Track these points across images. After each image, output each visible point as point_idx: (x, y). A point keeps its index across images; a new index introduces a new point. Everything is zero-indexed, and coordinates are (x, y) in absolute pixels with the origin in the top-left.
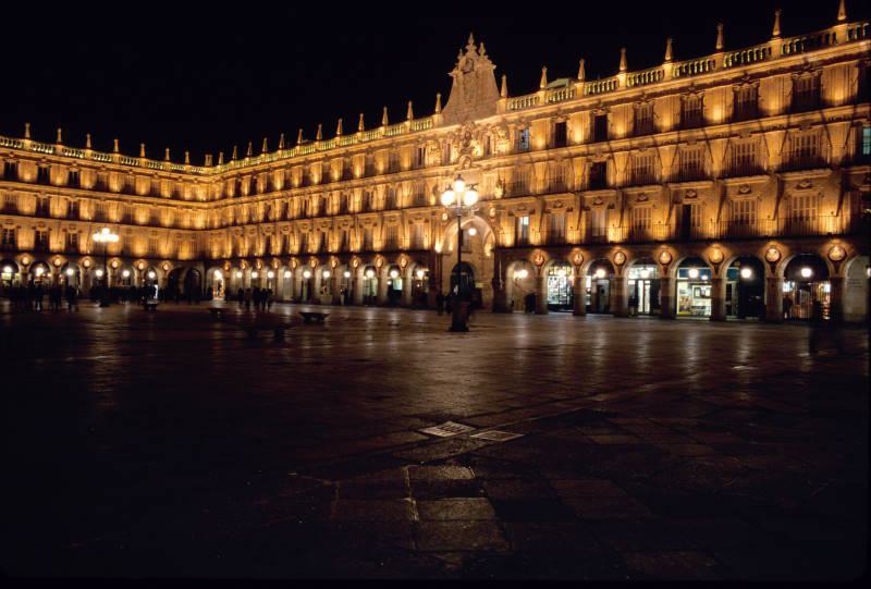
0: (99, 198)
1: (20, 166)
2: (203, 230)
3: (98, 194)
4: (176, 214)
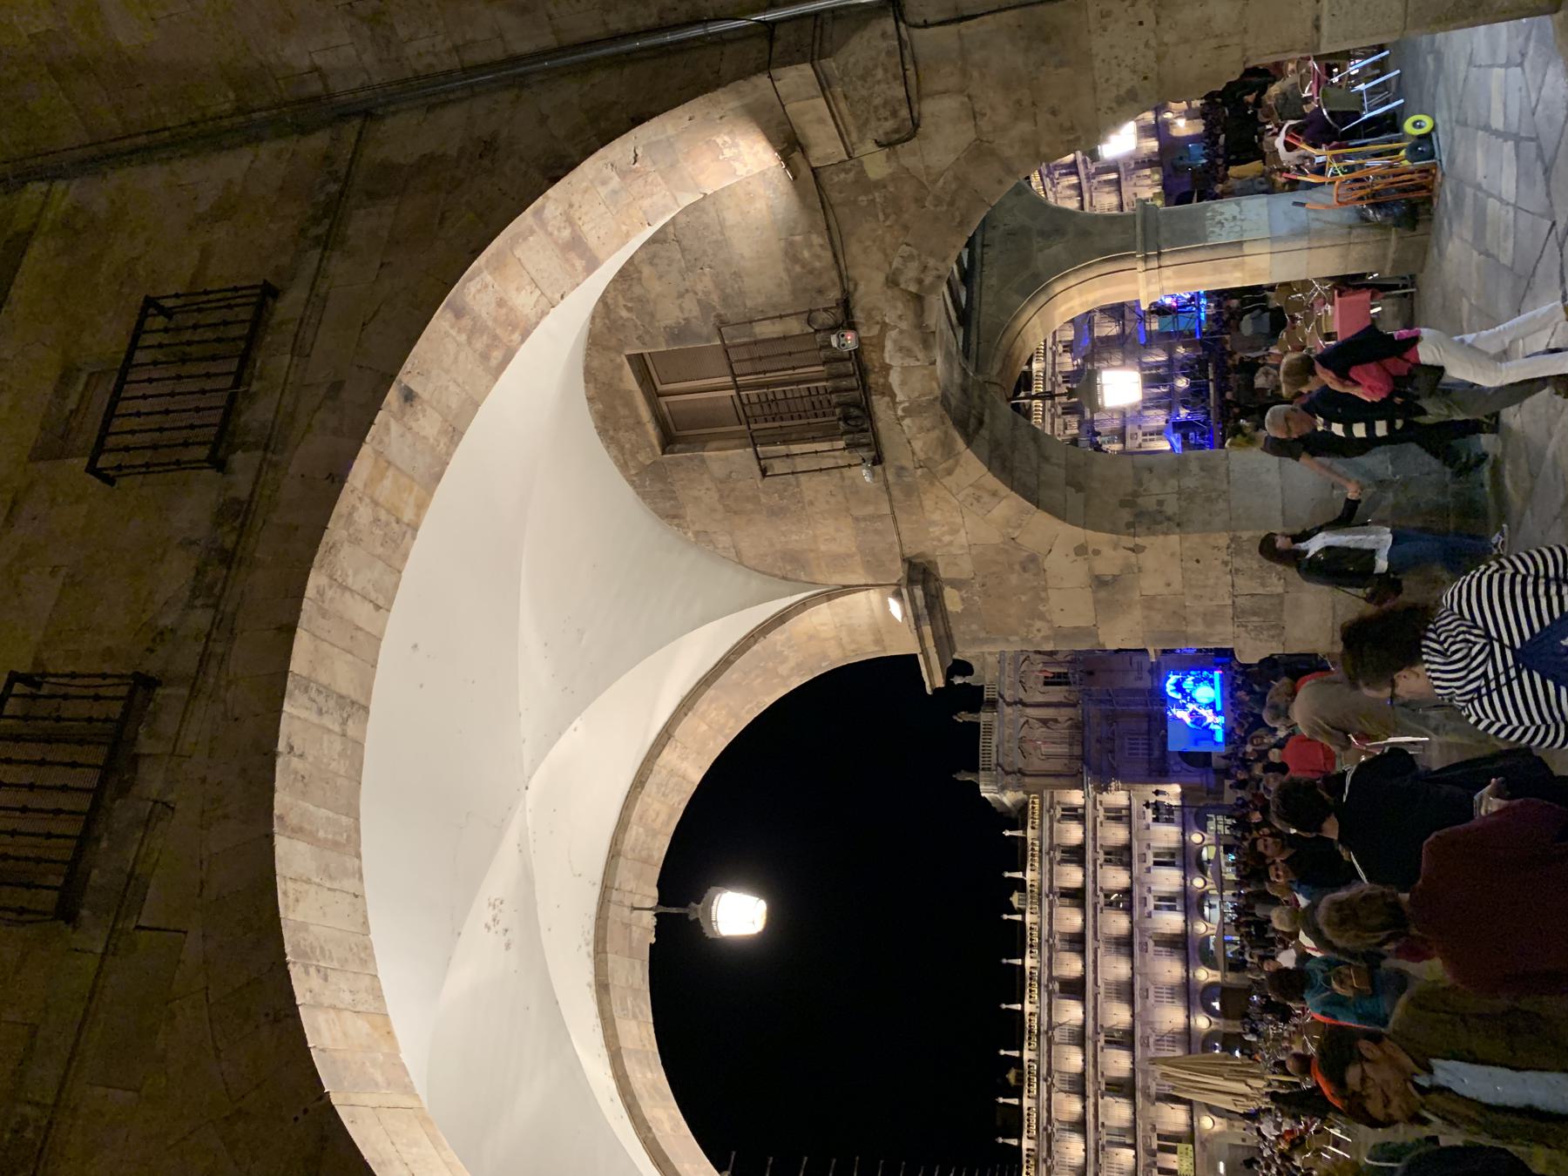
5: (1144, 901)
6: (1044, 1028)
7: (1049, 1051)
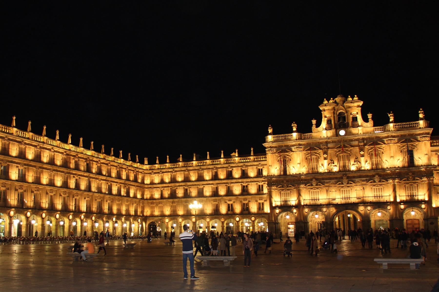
5: (230, 200)
6: (189, 168)
7: (182, 171)
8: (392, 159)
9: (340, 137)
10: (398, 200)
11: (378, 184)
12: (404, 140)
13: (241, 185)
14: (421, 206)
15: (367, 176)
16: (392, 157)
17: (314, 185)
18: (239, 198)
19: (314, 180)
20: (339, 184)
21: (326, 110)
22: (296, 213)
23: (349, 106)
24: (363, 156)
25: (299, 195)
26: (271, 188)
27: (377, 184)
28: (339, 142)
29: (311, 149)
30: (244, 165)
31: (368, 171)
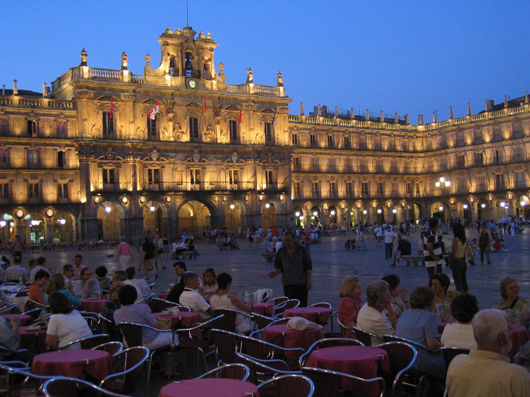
0: (362, 156)
1: (318, 137)
2: (422, 174)
3: (362, 153)
4: (406, 163)
8: (253, 132)
9: (189, 90)
10: (258, 189)
11: (235, 165)
12: (265, 109)
13: (26, 148)
14: (279, 197)
15: (222, 152)
16: (253, 129)
17: (154, 159)
18: (23, 174)
19: (155, 151)
20: (189, 161)
21: (170, 44)
22: (126, 203)
23: (202, 46)
24: (218, 123)
25: (135, 175)
26: (89, 159)
27: (235, 165)
28: (189, 96)
29: (150, 102)
30: (32, 112)
31: (227, 145)
